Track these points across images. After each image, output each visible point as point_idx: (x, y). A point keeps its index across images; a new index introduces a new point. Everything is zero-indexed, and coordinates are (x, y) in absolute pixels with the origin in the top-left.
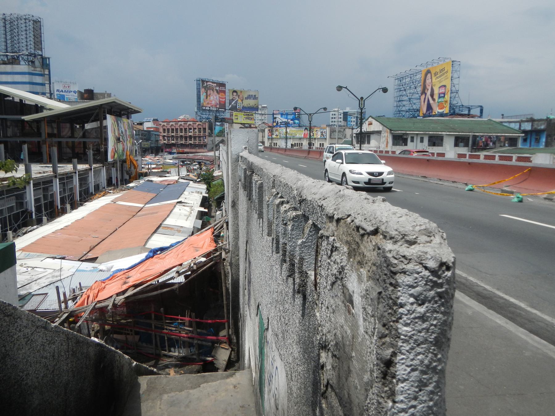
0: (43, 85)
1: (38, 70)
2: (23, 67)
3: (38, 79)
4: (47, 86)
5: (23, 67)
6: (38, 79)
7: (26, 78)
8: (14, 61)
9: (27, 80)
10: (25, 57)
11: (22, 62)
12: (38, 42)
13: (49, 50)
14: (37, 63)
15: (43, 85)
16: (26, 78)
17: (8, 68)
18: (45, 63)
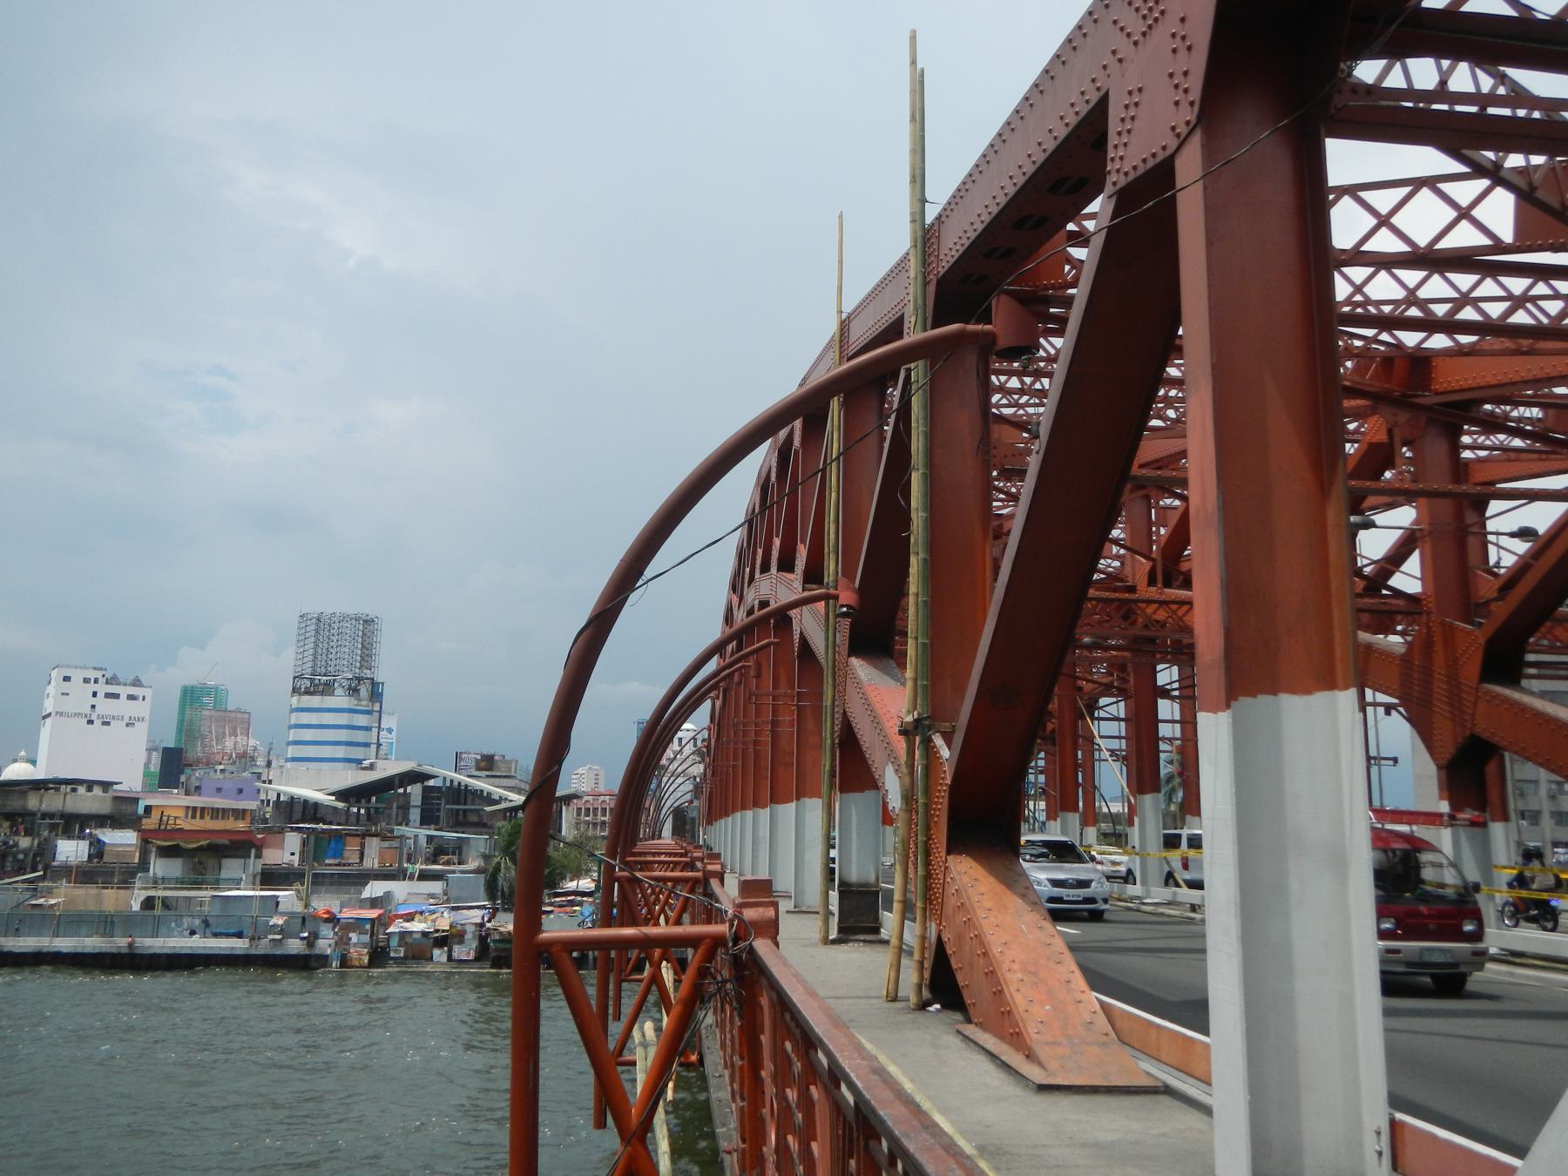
0: (368, 729)
1: (365, 704)
2: (340, 700)
3: (362, 720)
4: (375, 731)
5: (340, 700)
6: (362, 720)
7: (343, 719)
8: (327, 689)
9: (345, 723)
10: (345, 683)
11: (339, 691)
12: (367, 655)
13: (383, 672)
14: (364, 691)
15: (368, 729)
16: (343, 719)
17: (315, 701)
18: (376, 695)
